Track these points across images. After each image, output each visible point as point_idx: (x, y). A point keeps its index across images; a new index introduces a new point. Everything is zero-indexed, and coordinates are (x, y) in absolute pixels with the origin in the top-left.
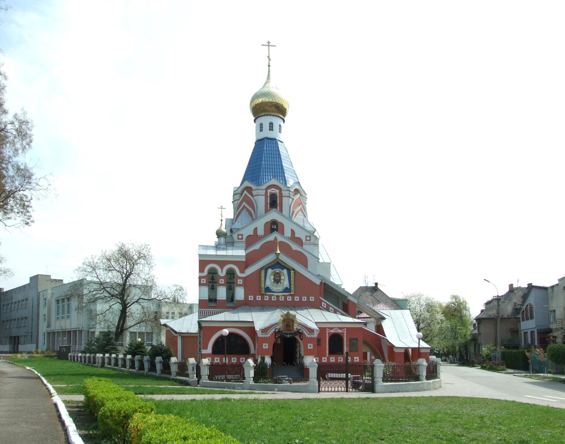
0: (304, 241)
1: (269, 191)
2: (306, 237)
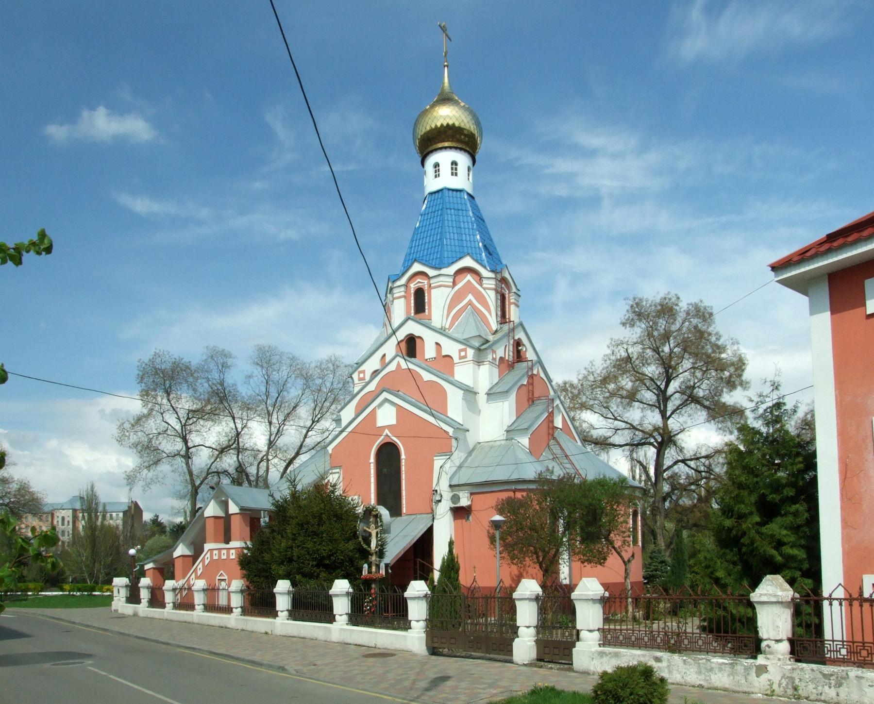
0: (456, 359)
1: (412, 285)
2: (460, 351)
